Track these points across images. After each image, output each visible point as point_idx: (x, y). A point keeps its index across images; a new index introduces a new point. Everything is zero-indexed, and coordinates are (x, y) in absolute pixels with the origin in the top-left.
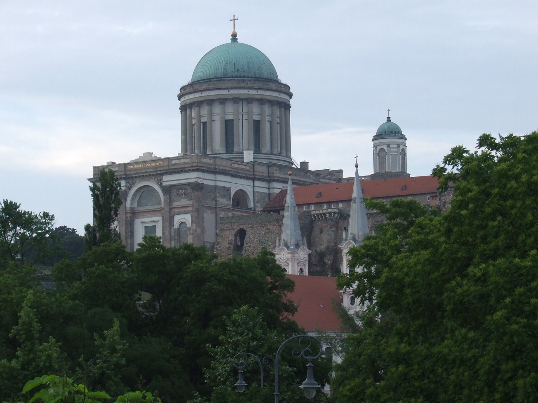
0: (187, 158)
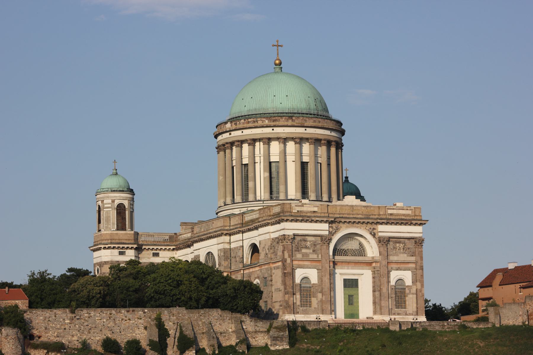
0: (407, 209)
